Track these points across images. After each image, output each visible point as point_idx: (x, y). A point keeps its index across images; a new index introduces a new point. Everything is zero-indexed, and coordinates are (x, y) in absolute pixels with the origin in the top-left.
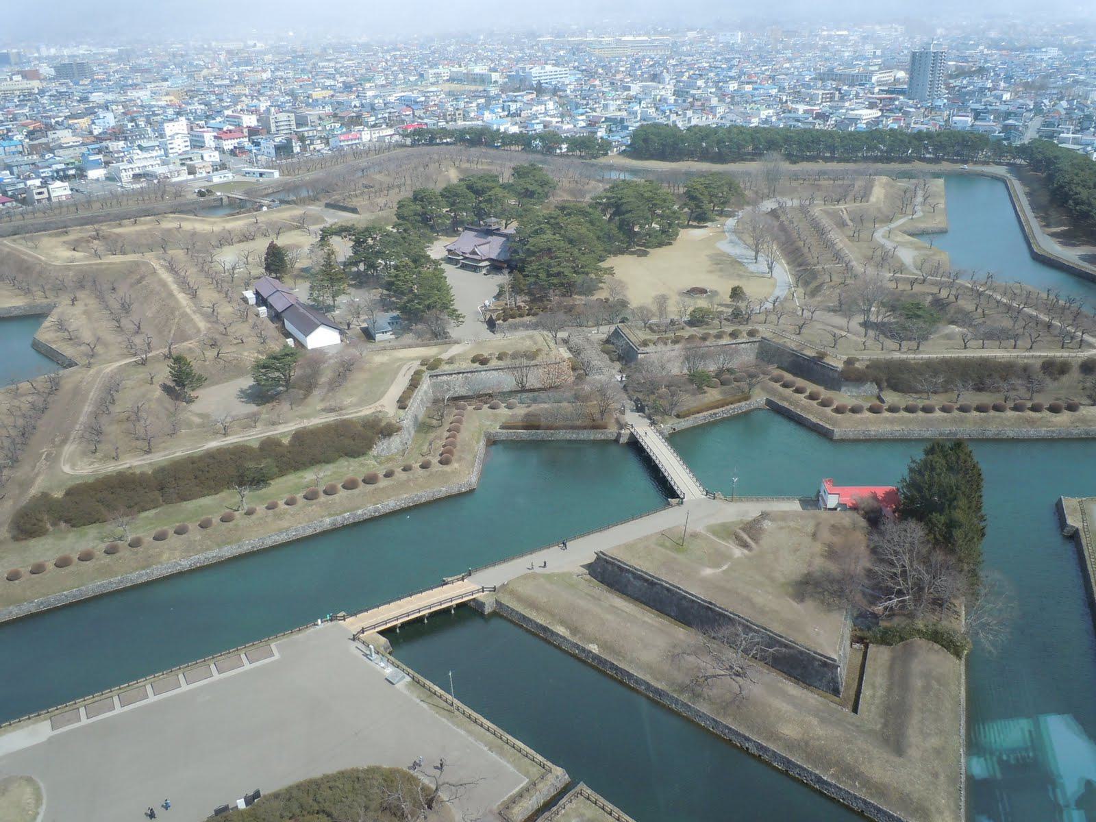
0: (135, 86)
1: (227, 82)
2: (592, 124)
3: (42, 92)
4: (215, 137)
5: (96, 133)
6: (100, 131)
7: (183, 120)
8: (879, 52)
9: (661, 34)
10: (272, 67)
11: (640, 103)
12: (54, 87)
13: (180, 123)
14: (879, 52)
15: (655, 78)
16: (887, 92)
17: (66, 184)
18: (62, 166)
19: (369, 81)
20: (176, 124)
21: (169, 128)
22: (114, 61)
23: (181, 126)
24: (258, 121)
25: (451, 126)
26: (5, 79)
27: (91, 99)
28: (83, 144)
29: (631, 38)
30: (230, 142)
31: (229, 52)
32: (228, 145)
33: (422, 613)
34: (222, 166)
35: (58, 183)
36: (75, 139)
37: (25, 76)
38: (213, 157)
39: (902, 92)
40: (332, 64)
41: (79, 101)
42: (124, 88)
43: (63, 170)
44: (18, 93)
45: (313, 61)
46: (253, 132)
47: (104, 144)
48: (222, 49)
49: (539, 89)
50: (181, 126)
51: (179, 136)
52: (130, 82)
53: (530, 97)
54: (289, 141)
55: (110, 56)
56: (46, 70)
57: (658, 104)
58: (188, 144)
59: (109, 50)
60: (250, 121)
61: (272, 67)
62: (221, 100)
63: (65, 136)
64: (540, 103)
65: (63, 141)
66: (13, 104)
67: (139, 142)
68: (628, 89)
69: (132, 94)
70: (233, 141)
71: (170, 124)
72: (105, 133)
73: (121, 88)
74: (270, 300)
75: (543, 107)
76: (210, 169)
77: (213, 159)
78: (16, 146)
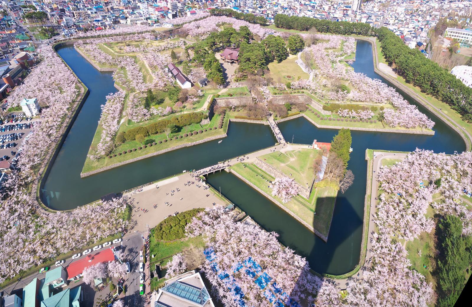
16: (346, 7)
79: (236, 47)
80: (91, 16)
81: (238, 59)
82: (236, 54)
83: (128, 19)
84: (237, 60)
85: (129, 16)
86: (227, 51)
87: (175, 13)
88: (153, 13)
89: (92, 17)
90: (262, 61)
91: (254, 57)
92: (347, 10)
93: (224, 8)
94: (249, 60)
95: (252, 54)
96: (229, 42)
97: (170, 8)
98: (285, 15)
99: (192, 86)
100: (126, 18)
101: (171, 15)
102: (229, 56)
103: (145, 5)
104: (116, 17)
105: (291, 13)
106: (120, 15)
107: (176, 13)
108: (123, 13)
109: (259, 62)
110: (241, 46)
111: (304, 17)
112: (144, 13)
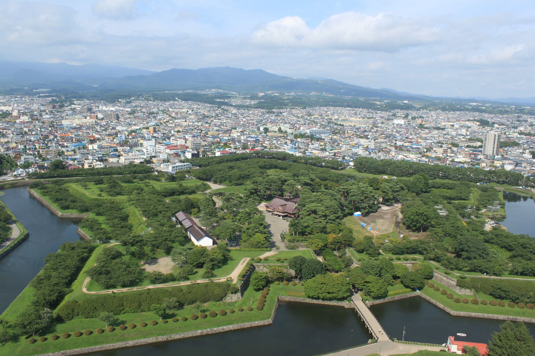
0: (135, 125)
1: (173, 125)
8: (468, 133)
9: (369, 118)
11: (359, 147)
12: (104, 123)
13: (153, 141)
14: (468, 133)
16: (473, 151)
17: (102, 163)
19: (235, 129)
22: (128, 114)
24: (186, 143)
27: (117, 128)
29: (354, 119)
30: (172, 151)
31: (177, 113)
32: (172, 152)
35: (99, 163)
38: (163, 156)
39: (481, 151)
40: (220, 121)
41: (111, 129)
42: (130, 125)
43: (101, 157)
45: (212, 119)
48: (174, 112)
49: (312, 137)
51: (151, 147)
52: (134, 123)
55: (127, 111)
56: (100, 116)
57: (367, 149)
59: (127, 109)
60: (181, 142)
62: (170, 132)
66: (85, 128)
70: (174, 151)
73: (129, 125)
79: (292, 197)
80: (66, 154)
81: (295, 212)
82: (291, 206)
83: (121, 157)
84: (294, 214)
85: (124, 154)
86: (277, 201)
87: (196, 152)
88: (162, 151)
89: (66, 155)
90: (337, 214)
91: (323, 208)
92: (475, 154)
94: (315, 212)
95: (319, 205)
96: (282, 191)
97: (190, 147)
98: (372, 158)
99: (213, 244)
100: (119, 156)
102: (281, 208)
103: (152, 143)
104: (103, 155)
105: (382, 156)
106: (110, 153)
108: (116, 150)
109: (332, 216)
110: (301, 196)
111: (403, 161)
112: (148, 150)
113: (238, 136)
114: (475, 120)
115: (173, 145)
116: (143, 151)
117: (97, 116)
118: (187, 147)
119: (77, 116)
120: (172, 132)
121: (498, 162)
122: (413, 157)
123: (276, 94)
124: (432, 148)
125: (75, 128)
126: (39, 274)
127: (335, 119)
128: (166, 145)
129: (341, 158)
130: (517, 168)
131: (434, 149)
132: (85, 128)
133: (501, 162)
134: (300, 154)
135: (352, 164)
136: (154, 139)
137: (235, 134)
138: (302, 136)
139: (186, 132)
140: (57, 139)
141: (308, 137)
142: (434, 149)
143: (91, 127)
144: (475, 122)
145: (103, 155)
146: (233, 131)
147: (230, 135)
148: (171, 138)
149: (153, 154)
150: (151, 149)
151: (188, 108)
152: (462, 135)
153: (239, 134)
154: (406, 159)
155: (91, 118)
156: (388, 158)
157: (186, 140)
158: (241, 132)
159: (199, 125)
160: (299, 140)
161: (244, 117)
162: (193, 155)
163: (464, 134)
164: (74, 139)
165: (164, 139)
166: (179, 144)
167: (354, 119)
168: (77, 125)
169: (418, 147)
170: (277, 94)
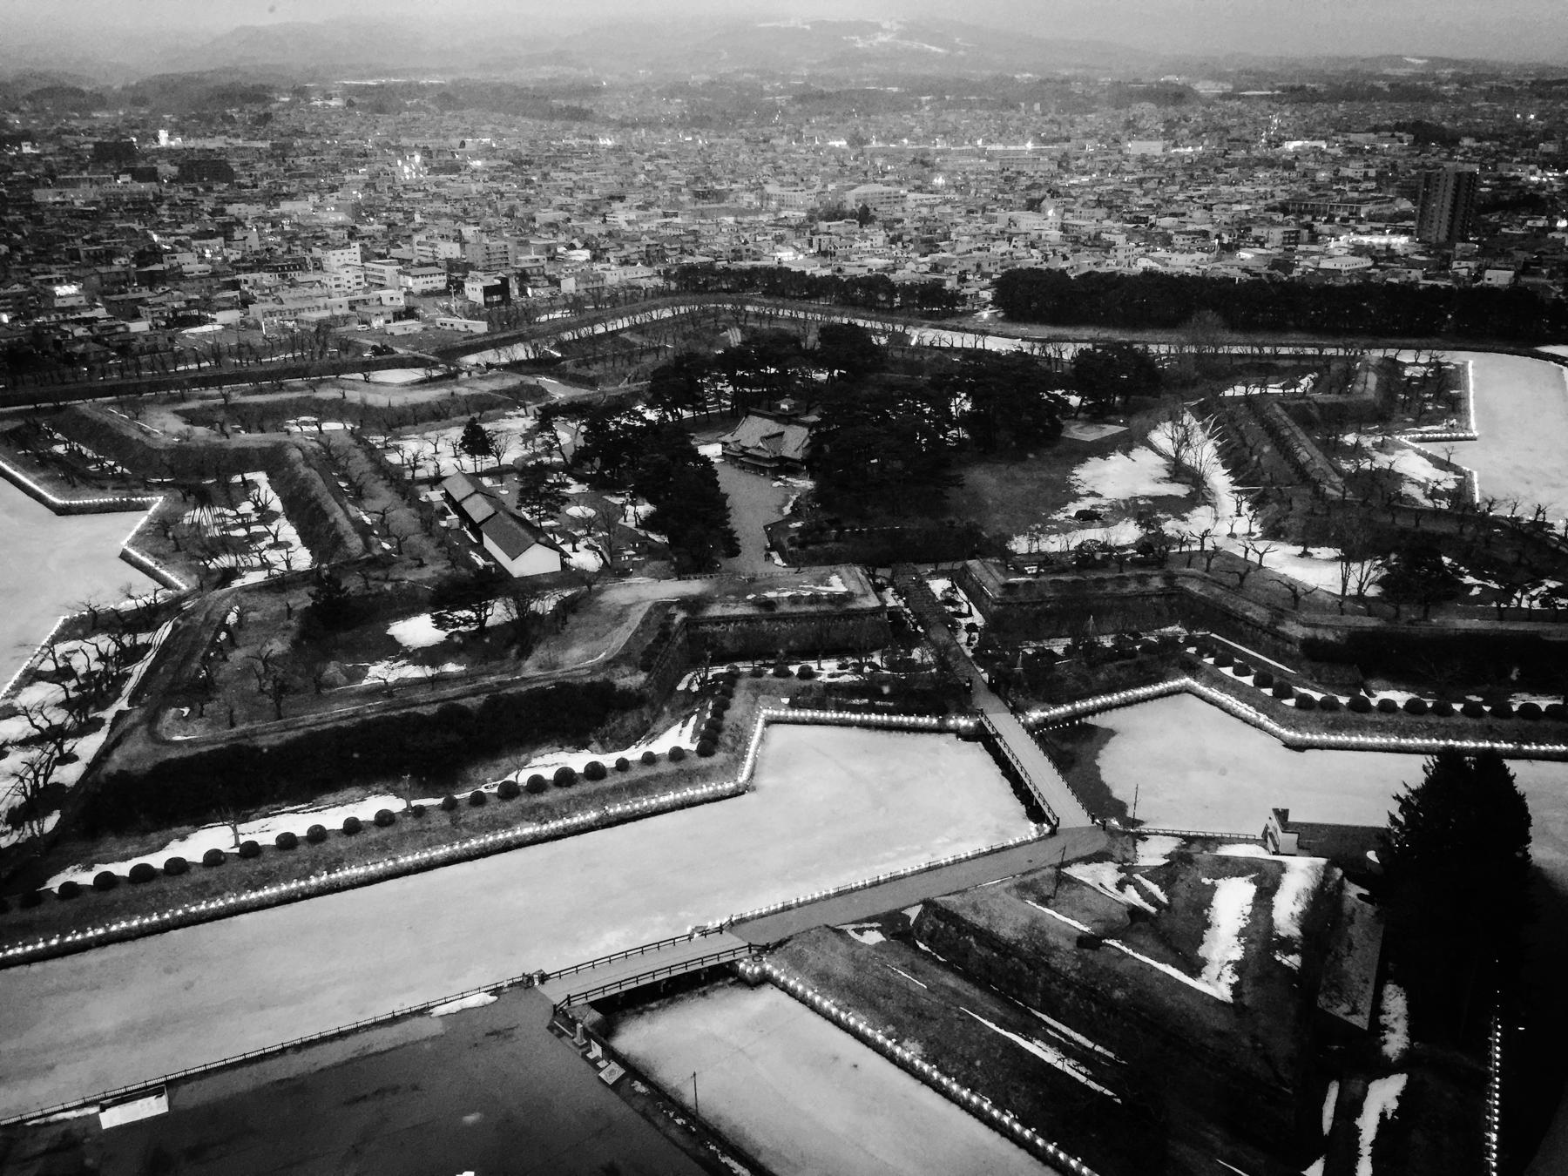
0: (289, 196)
1: (420, 195)
2: (935, 268)
3: (159, 199)
4: (400, 272)
5: (232, 258)
6: (239, 257)
7: (356, 247)
8: (1372, 173)
10: (486, 176)
11: (1010, 240)
13: (352, 250)
15: (1034, 205)
18: (183, 304)
19: (621, 199)
20: (346, 251)
21: (334, 259)
23: (354, 252)
25: (736, 265)
26: (109, 179)
28: (214, 274)
29: (1000, 147)
33: (658, 978)
34: (409, 313)
36: (202, 267)
37: (139, 176)
42: (274, 197)
44: (125, 198)
46: (452, 265)
47: (242, 277)
49: (864, 217)
50: (354, 252)
51: (349, 269)
52: (285, 189)
53: (850, 227)
54: (505, 281)
58: (362, 280)
59: (259, 144)
60: (450, 250)
61: (486, 176)
63: (189, 262)
64: (865, 238)
65: (185, 268)
67: (291, 274)
68: (992, 220)
69: (286, 206)
71: (338, 252)
72: (243, 260)
74: (466, 505)
75: (868, 243)
76: (390, 317)
77: (394, 303)
78: (118, 273)
87: (498, 282)
93: (747, 264)
101: (479, 286)
103: (352, 256)
105: (1084, 263)
107: (505, 281)
111: (1148, 274)
113: (629, 222)
114: (1399, 127)
115: (424, 260)
116: (322, 285)
117: (155, 169)
118: (467, 267)
119: (85, 174)
120: (418, 218)
121: (1464, 264)
122: (1182, 262)
123: (746, 75)
124: (1249, 229)
125: (82, 215)
126: (1232, 675)
127: (939, 153)
128: (401, 261)
129: (955, 279)
130: (1525, 280)
131: (1256, 232)
132: (117, 215)
133: (1472, 264)
134: (827, 272)
135: (987, 295)
136: (357, 244)
137: (621, 217)
138: (835, 214)
139: (464, 217)
140: (25, 257)
141: (853, 215)
142: (1256, 232)
143: (142, 208)
144: (1397, 134)
145: (188, 302)
146: (616, 205)
147: (605, 221)
148: (416, 238)
149: (360, 296)
150: (350, 276)
151: (462, 134)
152: (1351, 180)
153: (632, 216)
154: (1161, 268)
155: (134, 178)
156: (1102, 269)
157: (460, 239)
158: (638, 207)
159: (503, 189)
160: (823, 225)
161: (650, 159)
162: (488, 291)
163: (1359, 176)
164: (82, 254)
165: (393, 244)
166: (441, 257)
167: (1000, 147)
168: (86, 204)
169: (1203, 227)
170: (753, 76)
